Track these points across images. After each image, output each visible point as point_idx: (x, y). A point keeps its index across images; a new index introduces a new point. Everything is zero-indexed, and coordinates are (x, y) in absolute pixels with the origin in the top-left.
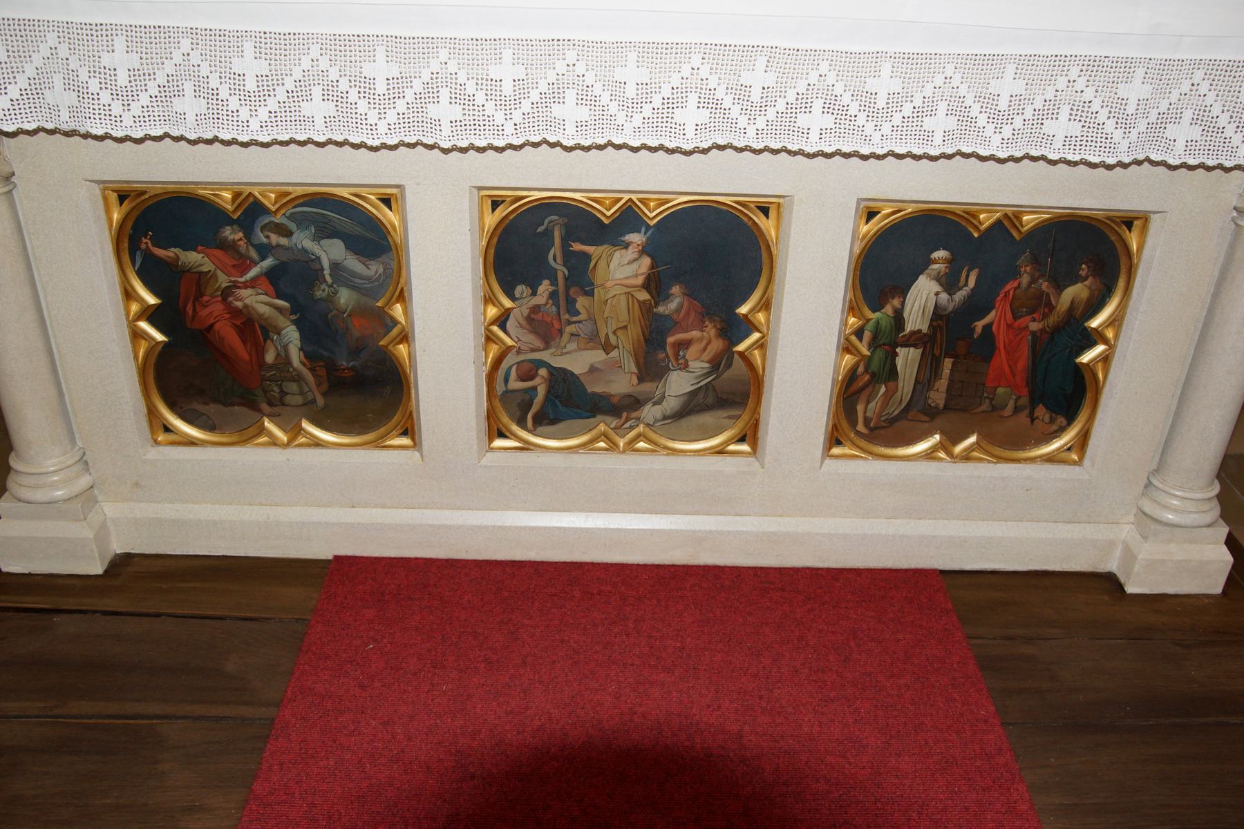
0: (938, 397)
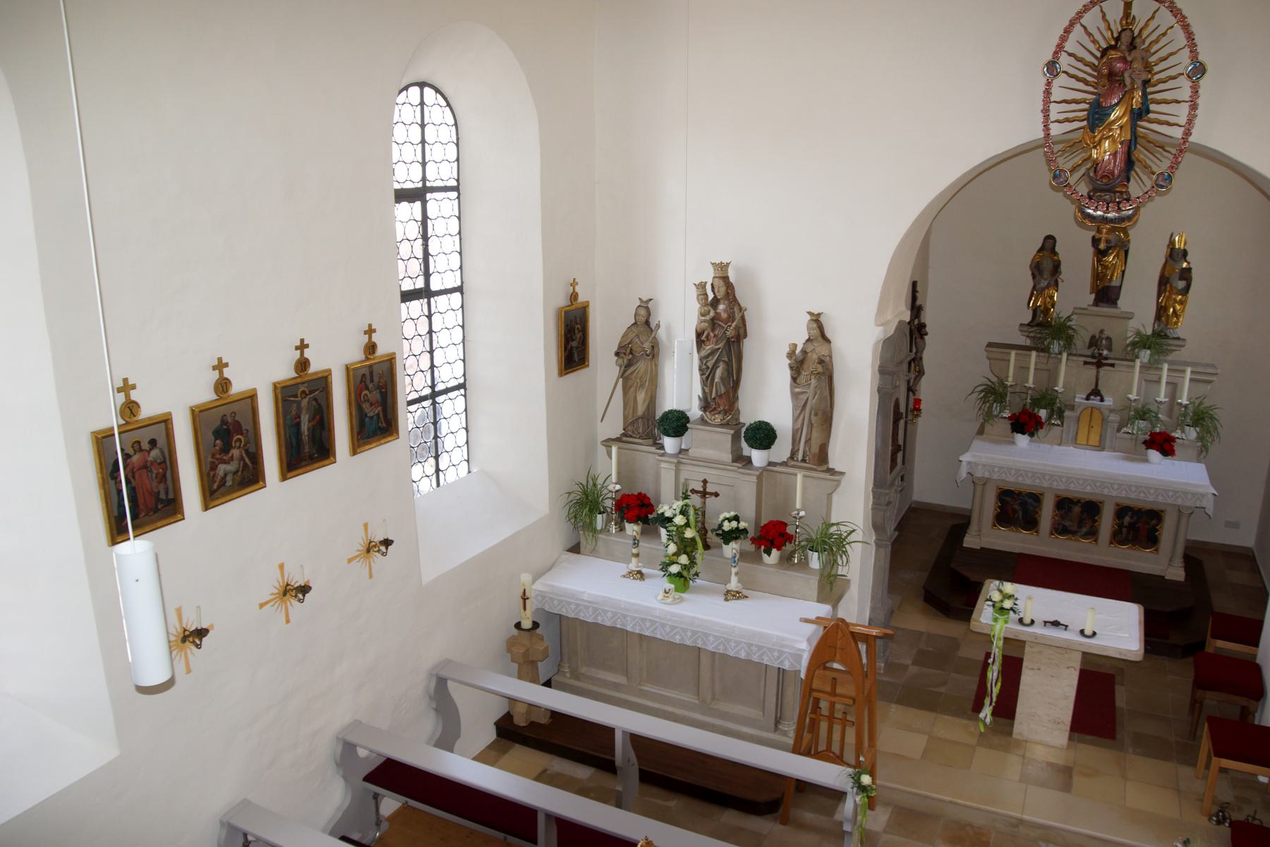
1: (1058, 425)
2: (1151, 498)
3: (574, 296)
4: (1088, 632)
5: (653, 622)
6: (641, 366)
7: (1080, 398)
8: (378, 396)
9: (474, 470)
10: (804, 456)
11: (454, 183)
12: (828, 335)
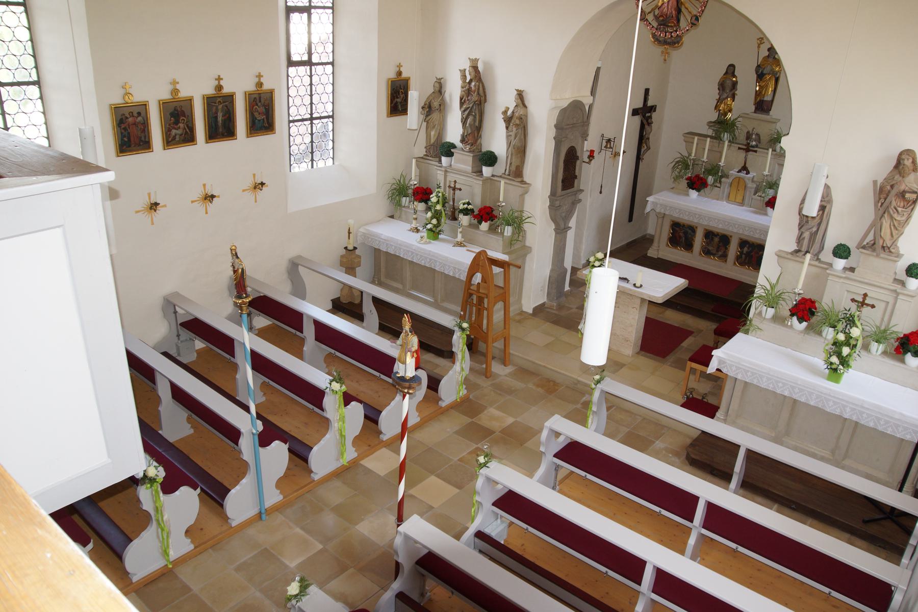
0: (747, 261)
1: (719, 187)
2: (757, 236)
3: (399, 73)
4: (638, 285)
5: (412, 253)
6: (435, 116)
7: (733, 173)
8: (264, 110)
9: (336, 163)
10: (509, 172)
11: (331, 5)
12: (526, 103)
